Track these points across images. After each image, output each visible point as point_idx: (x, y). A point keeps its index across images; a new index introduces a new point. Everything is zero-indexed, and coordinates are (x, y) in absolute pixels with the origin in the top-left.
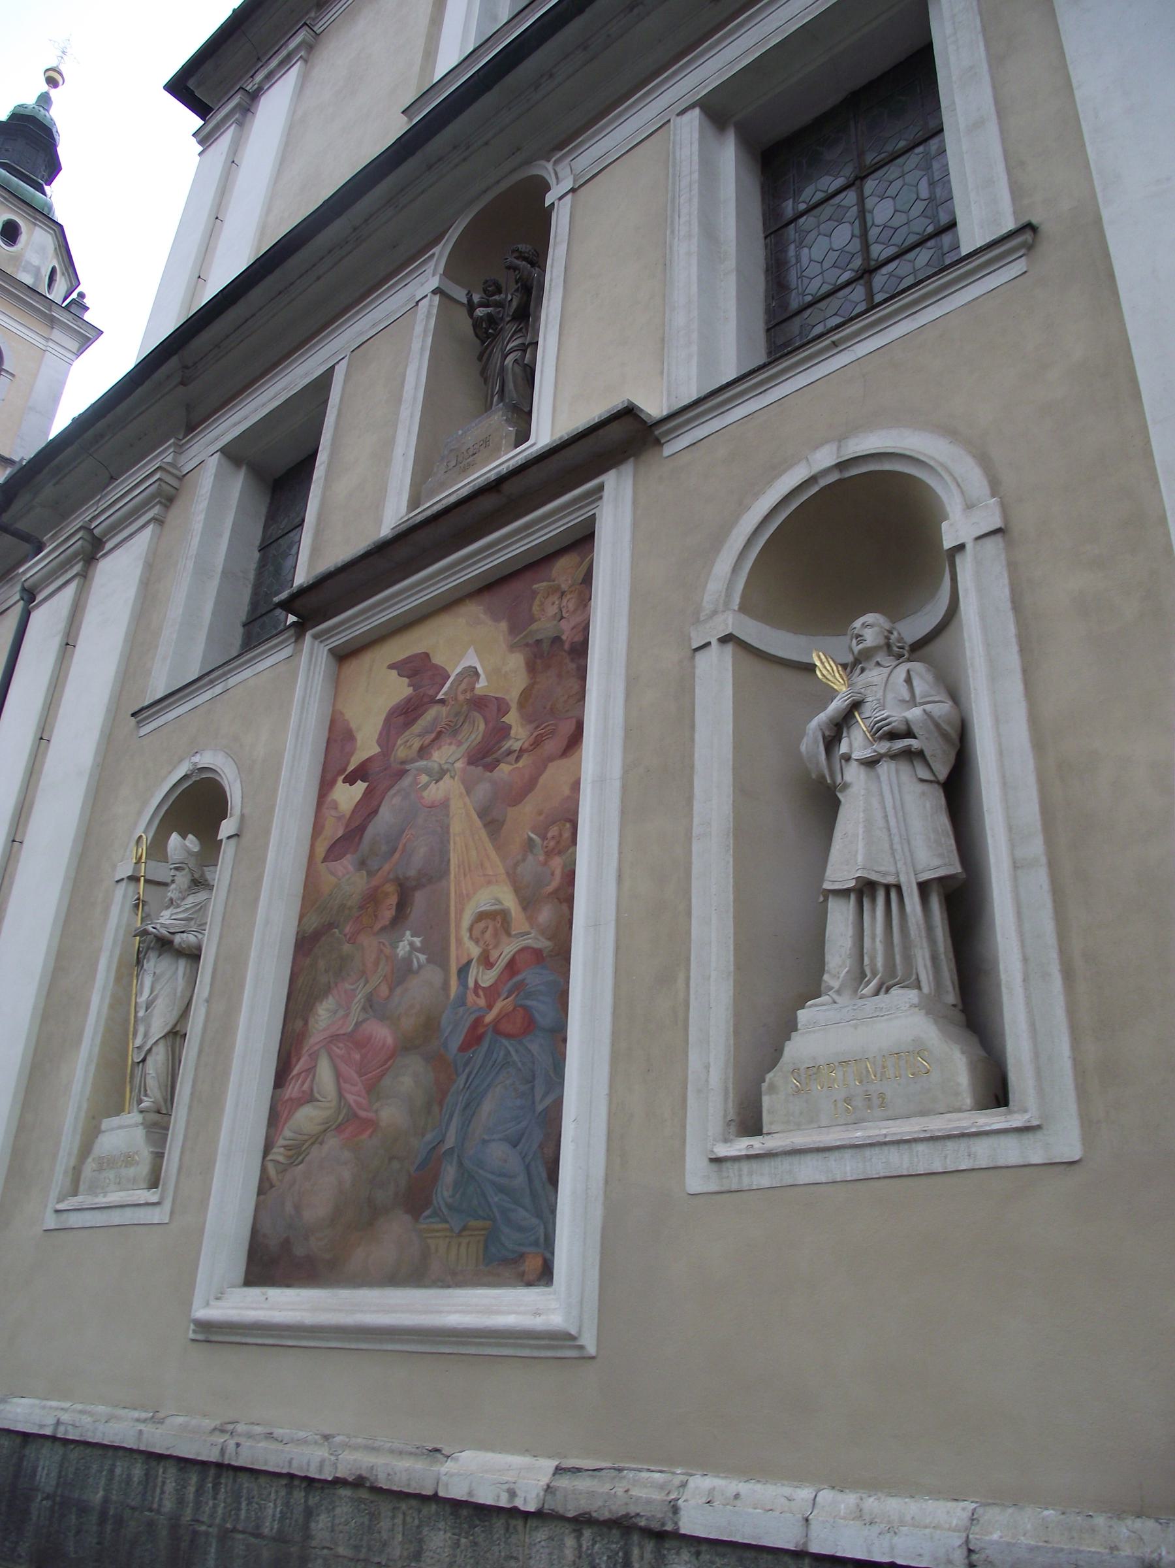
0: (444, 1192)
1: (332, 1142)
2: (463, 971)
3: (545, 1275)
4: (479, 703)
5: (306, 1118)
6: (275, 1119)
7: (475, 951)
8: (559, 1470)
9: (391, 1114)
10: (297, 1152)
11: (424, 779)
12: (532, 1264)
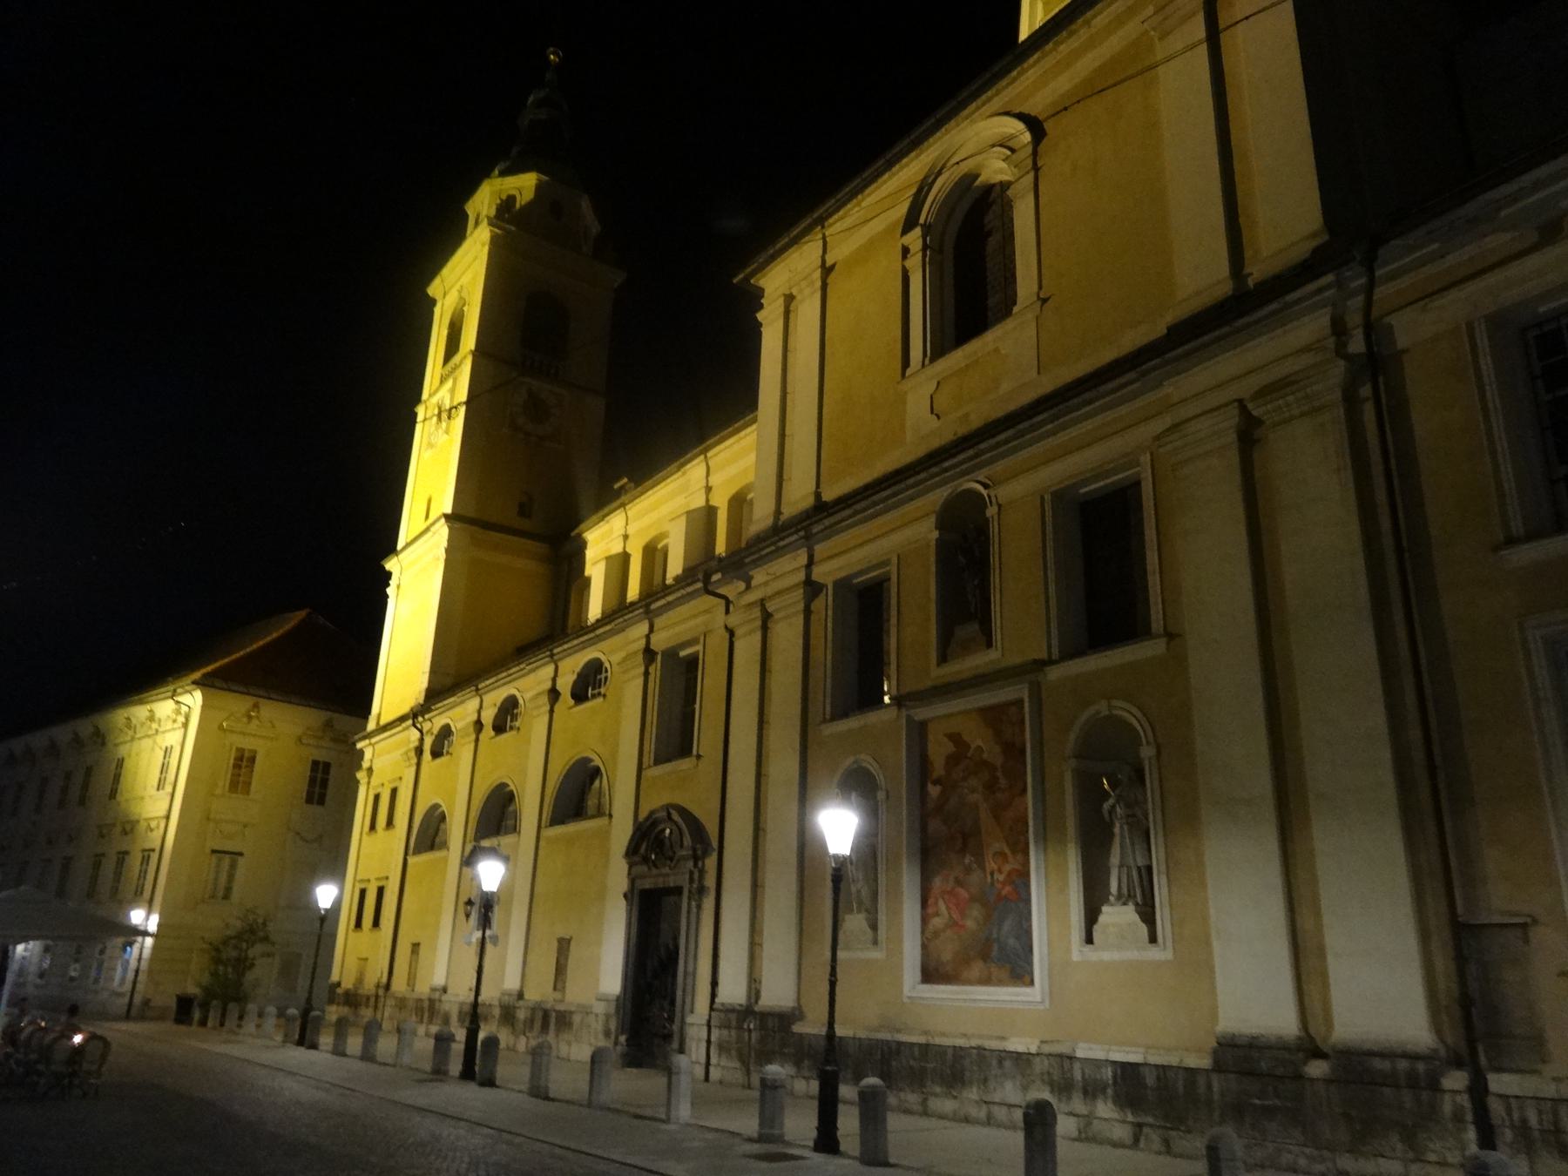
0: (995, 953)
1: (949, 933)
2: (992, 874)
3: (1032, 983)
4: (985, 763)
5: (937, 922)
6: (925, 920)
7: (996, 867)
8: (1042, 1042)
9: (970, 924)
10: (936, 934)
11: (966, 791)
12: (1027, 979)
